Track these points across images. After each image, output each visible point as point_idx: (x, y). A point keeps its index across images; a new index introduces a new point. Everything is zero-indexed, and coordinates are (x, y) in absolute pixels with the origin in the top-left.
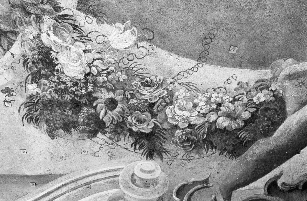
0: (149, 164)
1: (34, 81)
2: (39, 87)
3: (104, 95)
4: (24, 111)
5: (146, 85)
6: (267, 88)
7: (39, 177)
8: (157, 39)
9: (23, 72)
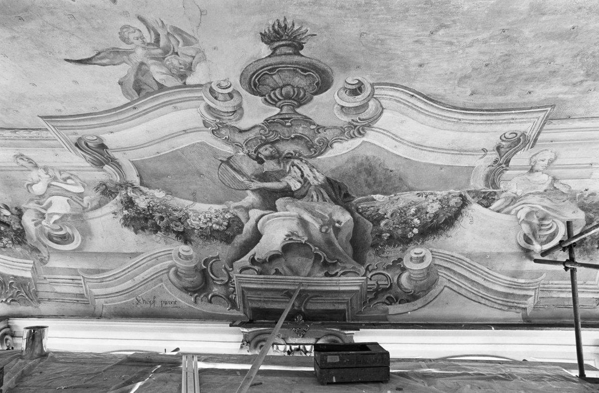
0: (186, 247)
1: (126, 209)
2: (128, 211)
3: (157, 215)
4: (122, 222)
5: (175, 210)
6: (229, 212)
7: (132, 253)
8: (174, 194)
9: (122, 206)
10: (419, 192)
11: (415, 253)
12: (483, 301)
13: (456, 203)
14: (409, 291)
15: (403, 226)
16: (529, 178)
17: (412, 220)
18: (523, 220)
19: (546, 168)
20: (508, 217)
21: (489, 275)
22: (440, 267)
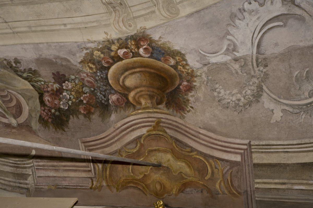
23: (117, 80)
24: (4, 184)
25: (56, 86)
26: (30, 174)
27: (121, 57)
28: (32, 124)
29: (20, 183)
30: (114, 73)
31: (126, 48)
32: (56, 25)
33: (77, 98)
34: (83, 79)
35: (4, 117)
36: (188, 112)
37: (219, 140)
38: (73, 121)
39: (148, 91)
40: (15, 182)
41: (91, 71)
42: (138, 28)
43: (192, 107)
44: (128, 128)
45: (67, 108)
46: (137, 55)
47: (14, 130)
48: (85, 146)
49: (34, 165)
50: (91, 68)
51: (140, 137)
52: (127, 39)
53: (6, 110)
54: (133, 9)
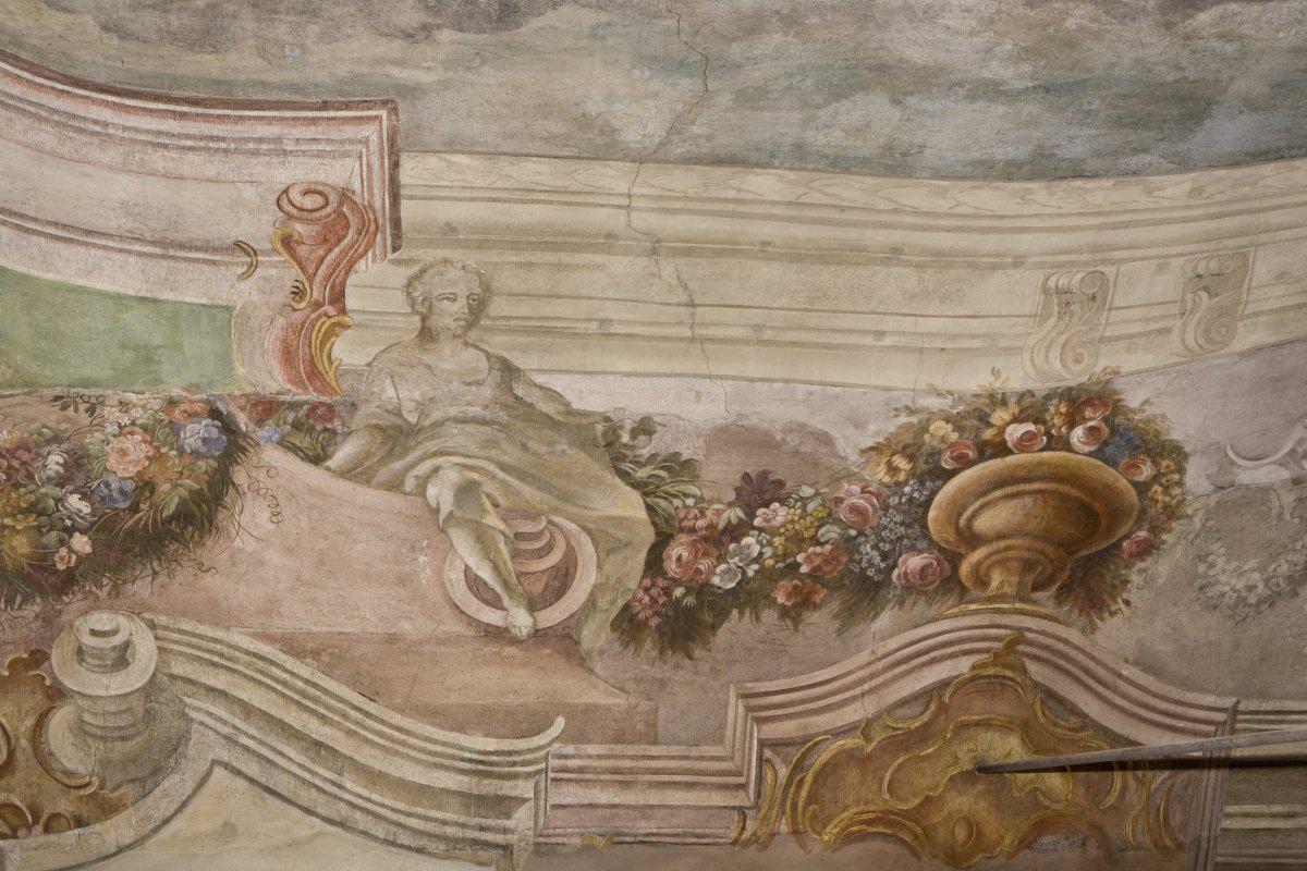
10: (58, 391)
11: (94, 633)
12: (361, 820)
13: (205, 440)
14: (80, 782)
15: (32, 520)
16: (425, 358)
17: (59, 500)
18: (451, 514)
19: (470, 326)
20: (396, 501)
21: (369, 722)
22: (190, 689)
23: (957, 507)
24: (422, 833)
25: (735, 514)
26: (527, 796)
27: (1010, 445)
28: (585, 632)
29: (482, 829)
30: (961, 490)
31: (1036, 422)
32: (851, 331)
33: (786, 555)
34: (839, 501)
35: (495, 603)
36: (1112, 614)
37: (1163, 698)
38: (737, 628)
39: (1029, 549)
40: (463, 826)
41: (887, 479)
42: (1098, 369)
43: (1127, 603)
44: (918, 655)
45: (733, 585)
46: (1060, 443)
47: (510, 650)
48: (749, 709)
49: (547, 768)
50: (892, 469)
51: (943, 685)
52: (1048, 397)
53: (514, 580)
54: (1116, 316)
